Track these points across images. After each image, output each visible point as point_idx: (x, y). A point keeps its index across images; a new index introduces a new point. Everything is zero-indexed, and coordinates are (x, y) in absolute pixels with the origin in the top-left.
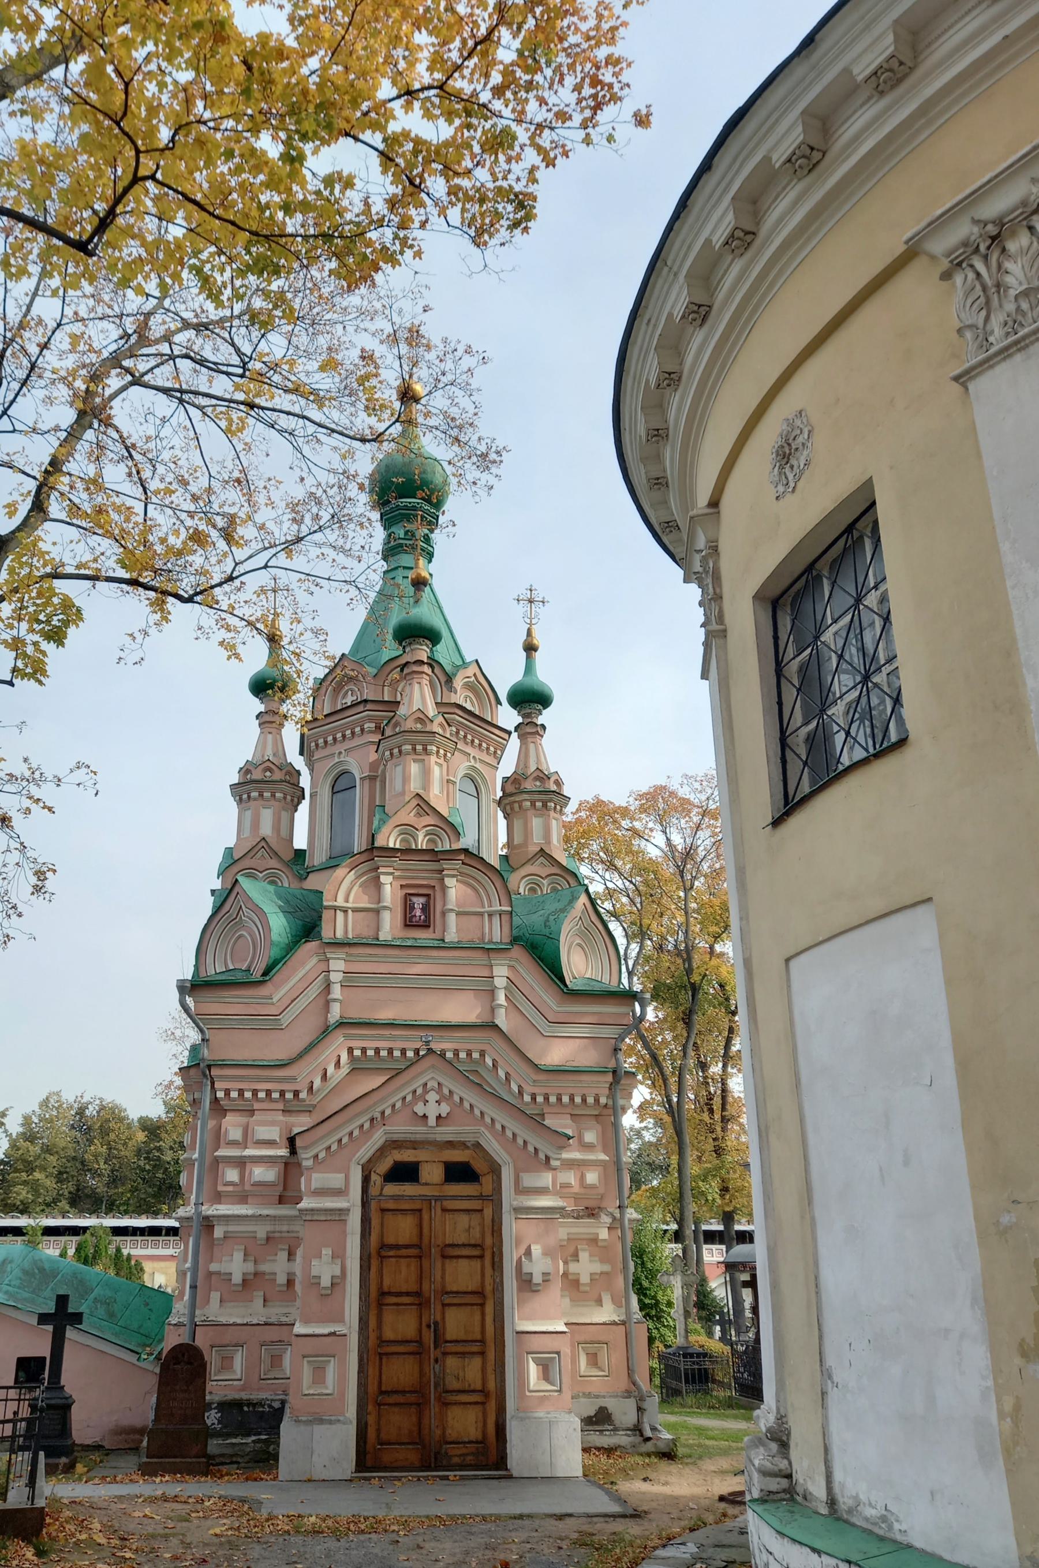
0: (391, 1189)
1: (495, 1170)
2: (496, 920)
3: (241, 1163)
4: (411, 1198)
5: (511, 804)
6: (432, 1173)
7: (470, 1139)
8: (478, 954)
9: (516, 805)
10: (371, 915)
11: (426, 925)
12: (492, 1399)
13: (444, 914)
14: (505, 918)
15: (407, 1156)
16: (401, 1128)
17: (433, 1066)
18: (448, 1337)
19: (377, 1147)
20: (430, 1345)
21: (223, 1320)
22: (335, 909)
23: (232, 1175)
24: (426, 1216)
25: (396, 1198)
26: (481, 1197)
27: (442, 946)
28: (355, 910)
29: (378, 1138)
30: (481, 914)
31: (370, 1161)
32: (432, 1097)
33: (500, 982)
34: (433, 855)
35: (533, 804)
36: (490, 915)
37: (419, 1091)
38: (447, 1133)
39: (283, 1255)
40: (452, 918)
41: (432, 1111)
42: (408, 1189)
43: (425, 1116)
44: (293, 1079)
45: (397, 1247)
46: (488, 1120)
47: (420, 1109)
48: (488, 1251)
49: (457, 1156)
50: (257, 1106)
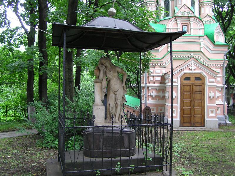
3: (153, 77)
4: (189, 83)
5: (201, 5)
6: (193, 79)
8: (198, 37)
9: (202, 5)
12: (203, 116)
13: (190, 29)
14: (203, 30)
16: (187, 71)
17: (193, 60)
18: (196, 106)
19: (182, 74)
20: (192, 108)
22: (169, 29)
23: (152, 78)
24: (192, 86)
25: (186, 83)
28: (172, 29)
29: (182, 73)
30: (198, 29)
31: (181, 77)
32: (193, 65)
33: (202, 43)
34: (189, 17)
35: (206, 4)
36: (200, 29)
37: (190, 64)
39: (161, 92)
40: (192, 30)
41: (193, 68)
43: (191, 69)
44: (162, 62)
46: (203, 69)
47: (190, 68)
48: (203, 92)
50: (155, 66)
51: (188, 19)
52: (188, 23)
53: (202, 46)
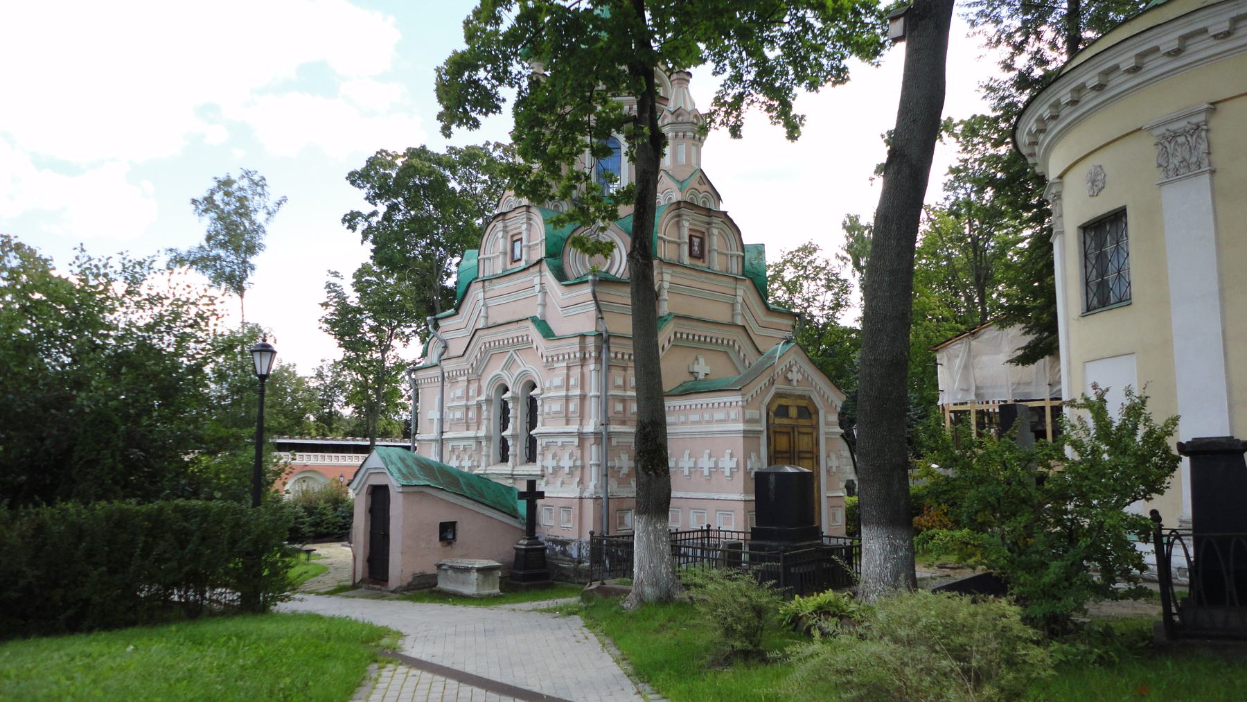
0: (778, 421)
1: (817, 412)
2: (735, 259)
4: (786, 426)
6: (793, 412)
7: (805, 393)
8: (731, 280)
10: (675, 246)
11: (701, 256)
15: (783, 402)
16: (780, 386)
21: (622, 495)
25: (780, 425)
26: (811, 426)
27: (709, 272)
28: (670, 242)
29: (773, 391)
33: (740, 300)
38: (799, 390)
40: (715, 256)
42: (785, 421)
45: (781, 452)
49: (803, 403)
51: (706, 219)
52: (704, 230)
53: (739, 307)
